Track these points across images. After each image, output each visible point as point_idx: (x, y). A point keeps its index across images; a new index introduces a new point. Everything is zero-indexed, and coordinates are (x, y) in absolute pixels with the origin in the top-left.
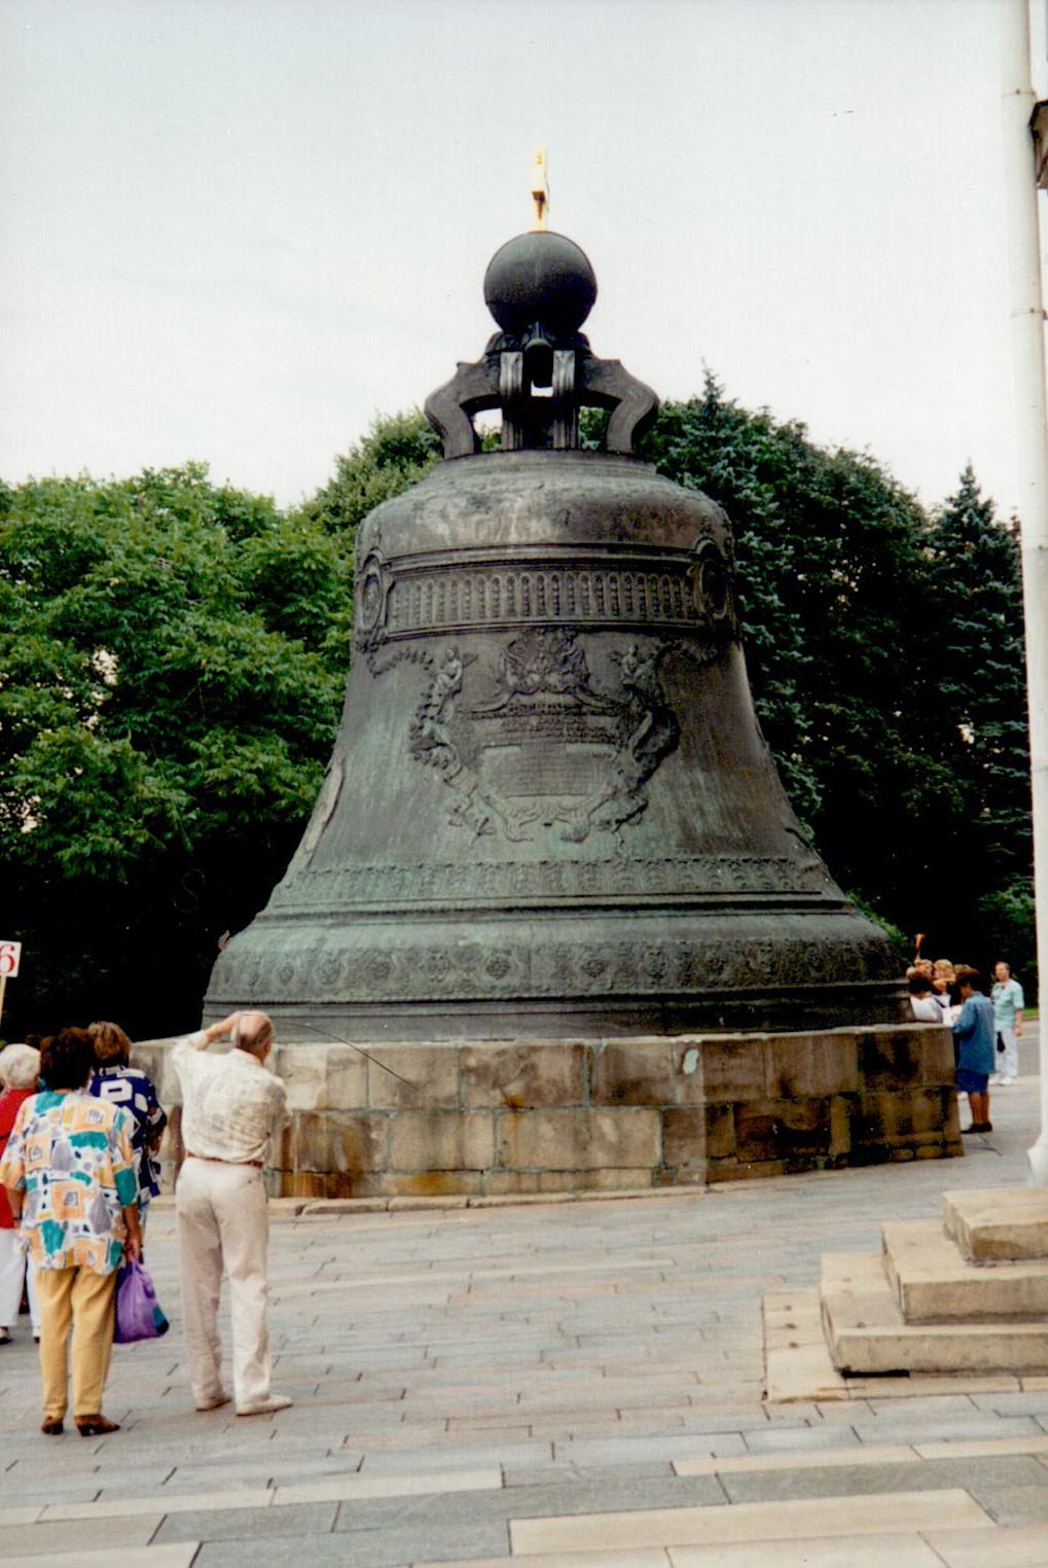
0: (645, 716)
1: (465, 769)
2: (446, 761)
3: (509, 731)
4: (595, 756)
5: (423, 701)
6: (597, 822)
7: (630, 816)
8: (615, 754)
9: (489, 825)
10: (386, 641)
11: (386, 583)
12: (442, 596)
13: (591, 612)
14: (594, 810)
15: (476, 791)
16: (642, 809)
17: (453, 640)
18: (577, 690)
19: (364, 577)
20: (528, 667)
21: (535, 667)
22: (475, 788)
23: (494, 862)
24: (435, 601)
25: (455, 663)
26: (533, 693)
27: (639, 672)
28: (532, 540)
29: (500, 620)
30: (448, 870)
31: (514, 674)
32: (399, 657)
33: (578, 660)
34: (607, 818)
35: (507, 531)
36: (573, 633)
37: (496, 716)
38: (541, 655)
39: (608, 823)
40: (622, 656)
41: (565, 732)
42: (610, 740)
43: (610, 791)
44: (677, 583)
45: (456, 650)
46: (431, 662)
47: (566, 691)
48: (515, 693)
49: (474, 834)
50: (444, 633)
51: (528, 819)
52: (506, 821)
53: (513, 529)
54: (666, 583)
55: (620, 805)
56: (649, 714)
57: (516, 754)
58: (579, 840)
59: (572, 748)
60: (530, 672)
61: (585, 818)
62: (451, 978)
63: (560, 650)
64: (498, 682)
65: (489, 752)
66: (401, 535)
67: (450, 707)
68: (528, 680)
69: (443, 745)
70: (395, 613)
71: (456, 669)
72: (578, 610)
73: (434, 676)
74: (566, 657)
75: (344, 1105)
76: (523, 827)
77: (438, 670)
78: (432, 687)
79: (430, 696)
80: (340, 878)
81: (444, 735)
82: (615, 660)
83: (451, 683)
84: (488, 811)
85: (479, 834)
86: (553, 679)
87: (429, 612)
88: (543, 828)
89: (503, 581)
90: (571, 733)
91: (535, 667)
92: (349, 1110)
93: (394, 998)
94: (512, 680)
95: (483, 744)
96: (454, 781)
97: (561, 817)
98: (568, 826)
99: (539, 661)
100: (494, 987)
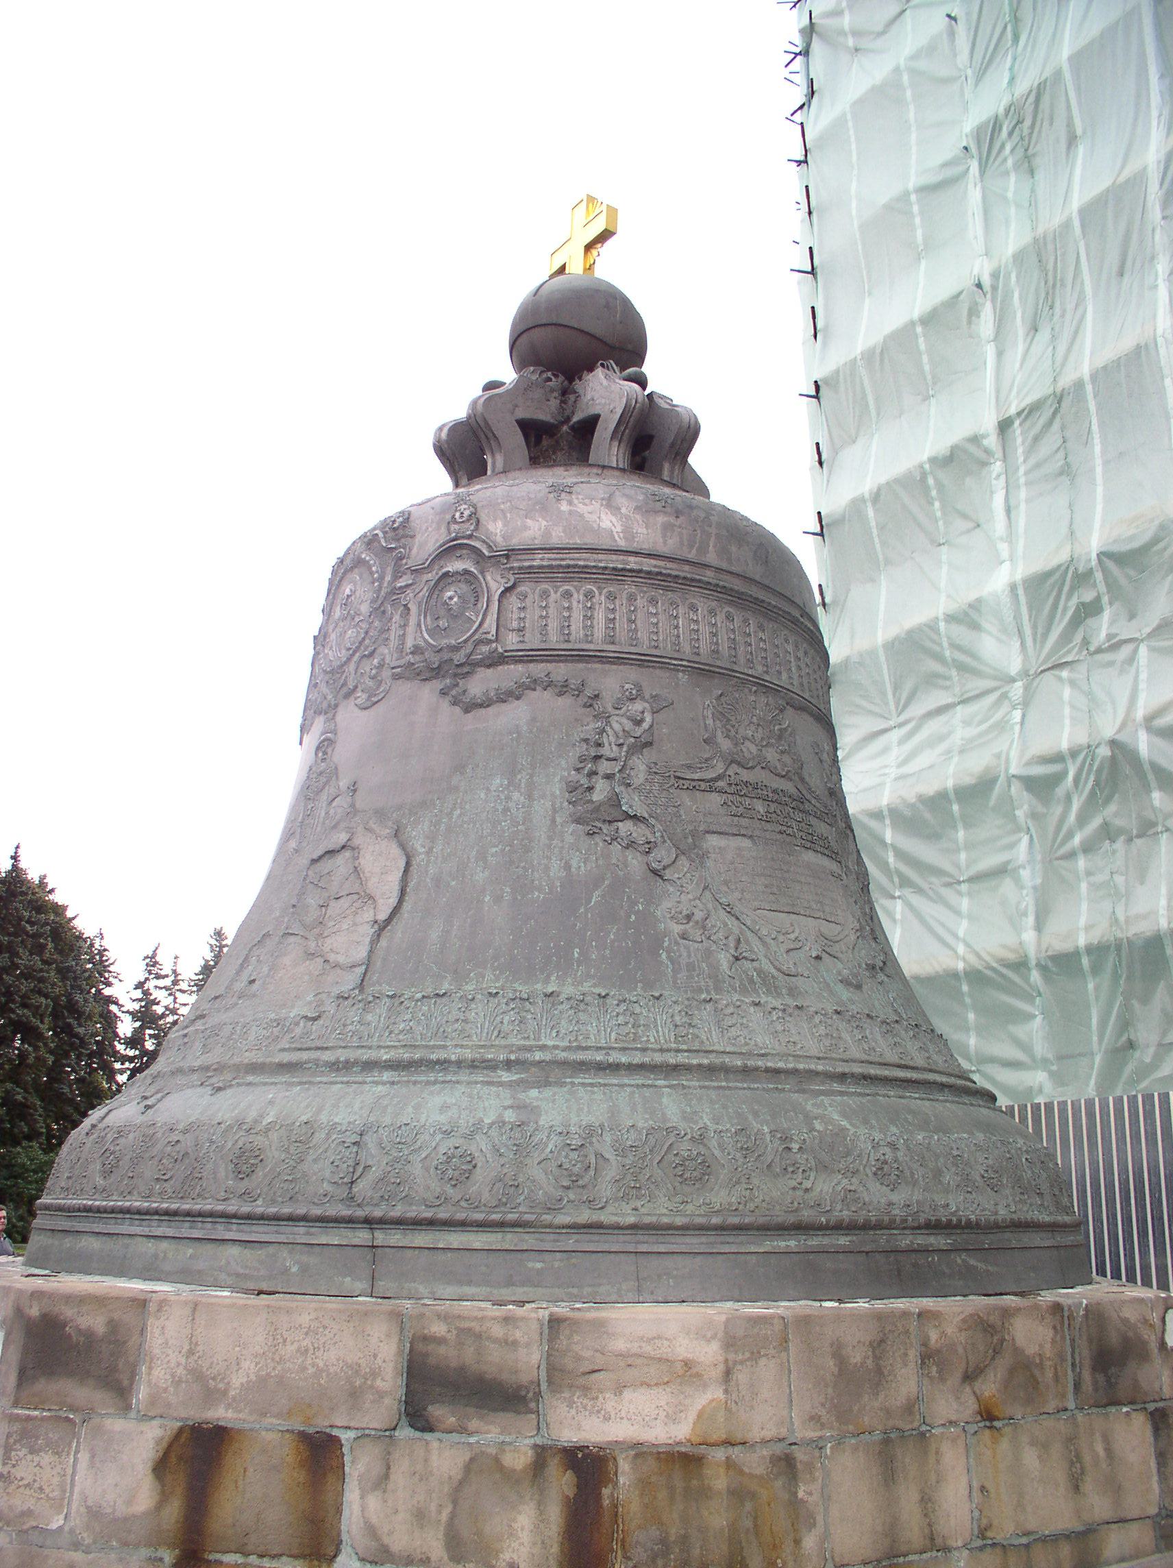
1: (683, 861)
9: (743, 946)
11: (494, 582)
12: (613, 610)
17: (631, 673)
18: (796, 778)
19: (432, 576)
21: (750, 733)
24: (600, 616)
25: (638, 706)
26: (752, 768)
28: (733, 569)
30: (709, 1007)
35: (703, 550)
37: (711, 790)
46: (597, 696)
48: (732, 762)
52: (765, 944)
59: (809, 856)
62: (824, 1187)
65: (713, 841)
66: (529, 522)
67: (639, 766)
68: (744, 750)
70: (515, 625)
71: (643, 712)
72: (784, 676)
75: (756, 1434)
77: (610, 709)
80: (478, 1011)
81: (633, 803)
83: (638, 732)
84: (731, 922)
85: (737, 959)
86: (771, 755)
91: (750, 733)
92: (765, 1442)
93: (735, 1220)
94: (725, 744)
97: (828, 950)
100: (890, 1204)
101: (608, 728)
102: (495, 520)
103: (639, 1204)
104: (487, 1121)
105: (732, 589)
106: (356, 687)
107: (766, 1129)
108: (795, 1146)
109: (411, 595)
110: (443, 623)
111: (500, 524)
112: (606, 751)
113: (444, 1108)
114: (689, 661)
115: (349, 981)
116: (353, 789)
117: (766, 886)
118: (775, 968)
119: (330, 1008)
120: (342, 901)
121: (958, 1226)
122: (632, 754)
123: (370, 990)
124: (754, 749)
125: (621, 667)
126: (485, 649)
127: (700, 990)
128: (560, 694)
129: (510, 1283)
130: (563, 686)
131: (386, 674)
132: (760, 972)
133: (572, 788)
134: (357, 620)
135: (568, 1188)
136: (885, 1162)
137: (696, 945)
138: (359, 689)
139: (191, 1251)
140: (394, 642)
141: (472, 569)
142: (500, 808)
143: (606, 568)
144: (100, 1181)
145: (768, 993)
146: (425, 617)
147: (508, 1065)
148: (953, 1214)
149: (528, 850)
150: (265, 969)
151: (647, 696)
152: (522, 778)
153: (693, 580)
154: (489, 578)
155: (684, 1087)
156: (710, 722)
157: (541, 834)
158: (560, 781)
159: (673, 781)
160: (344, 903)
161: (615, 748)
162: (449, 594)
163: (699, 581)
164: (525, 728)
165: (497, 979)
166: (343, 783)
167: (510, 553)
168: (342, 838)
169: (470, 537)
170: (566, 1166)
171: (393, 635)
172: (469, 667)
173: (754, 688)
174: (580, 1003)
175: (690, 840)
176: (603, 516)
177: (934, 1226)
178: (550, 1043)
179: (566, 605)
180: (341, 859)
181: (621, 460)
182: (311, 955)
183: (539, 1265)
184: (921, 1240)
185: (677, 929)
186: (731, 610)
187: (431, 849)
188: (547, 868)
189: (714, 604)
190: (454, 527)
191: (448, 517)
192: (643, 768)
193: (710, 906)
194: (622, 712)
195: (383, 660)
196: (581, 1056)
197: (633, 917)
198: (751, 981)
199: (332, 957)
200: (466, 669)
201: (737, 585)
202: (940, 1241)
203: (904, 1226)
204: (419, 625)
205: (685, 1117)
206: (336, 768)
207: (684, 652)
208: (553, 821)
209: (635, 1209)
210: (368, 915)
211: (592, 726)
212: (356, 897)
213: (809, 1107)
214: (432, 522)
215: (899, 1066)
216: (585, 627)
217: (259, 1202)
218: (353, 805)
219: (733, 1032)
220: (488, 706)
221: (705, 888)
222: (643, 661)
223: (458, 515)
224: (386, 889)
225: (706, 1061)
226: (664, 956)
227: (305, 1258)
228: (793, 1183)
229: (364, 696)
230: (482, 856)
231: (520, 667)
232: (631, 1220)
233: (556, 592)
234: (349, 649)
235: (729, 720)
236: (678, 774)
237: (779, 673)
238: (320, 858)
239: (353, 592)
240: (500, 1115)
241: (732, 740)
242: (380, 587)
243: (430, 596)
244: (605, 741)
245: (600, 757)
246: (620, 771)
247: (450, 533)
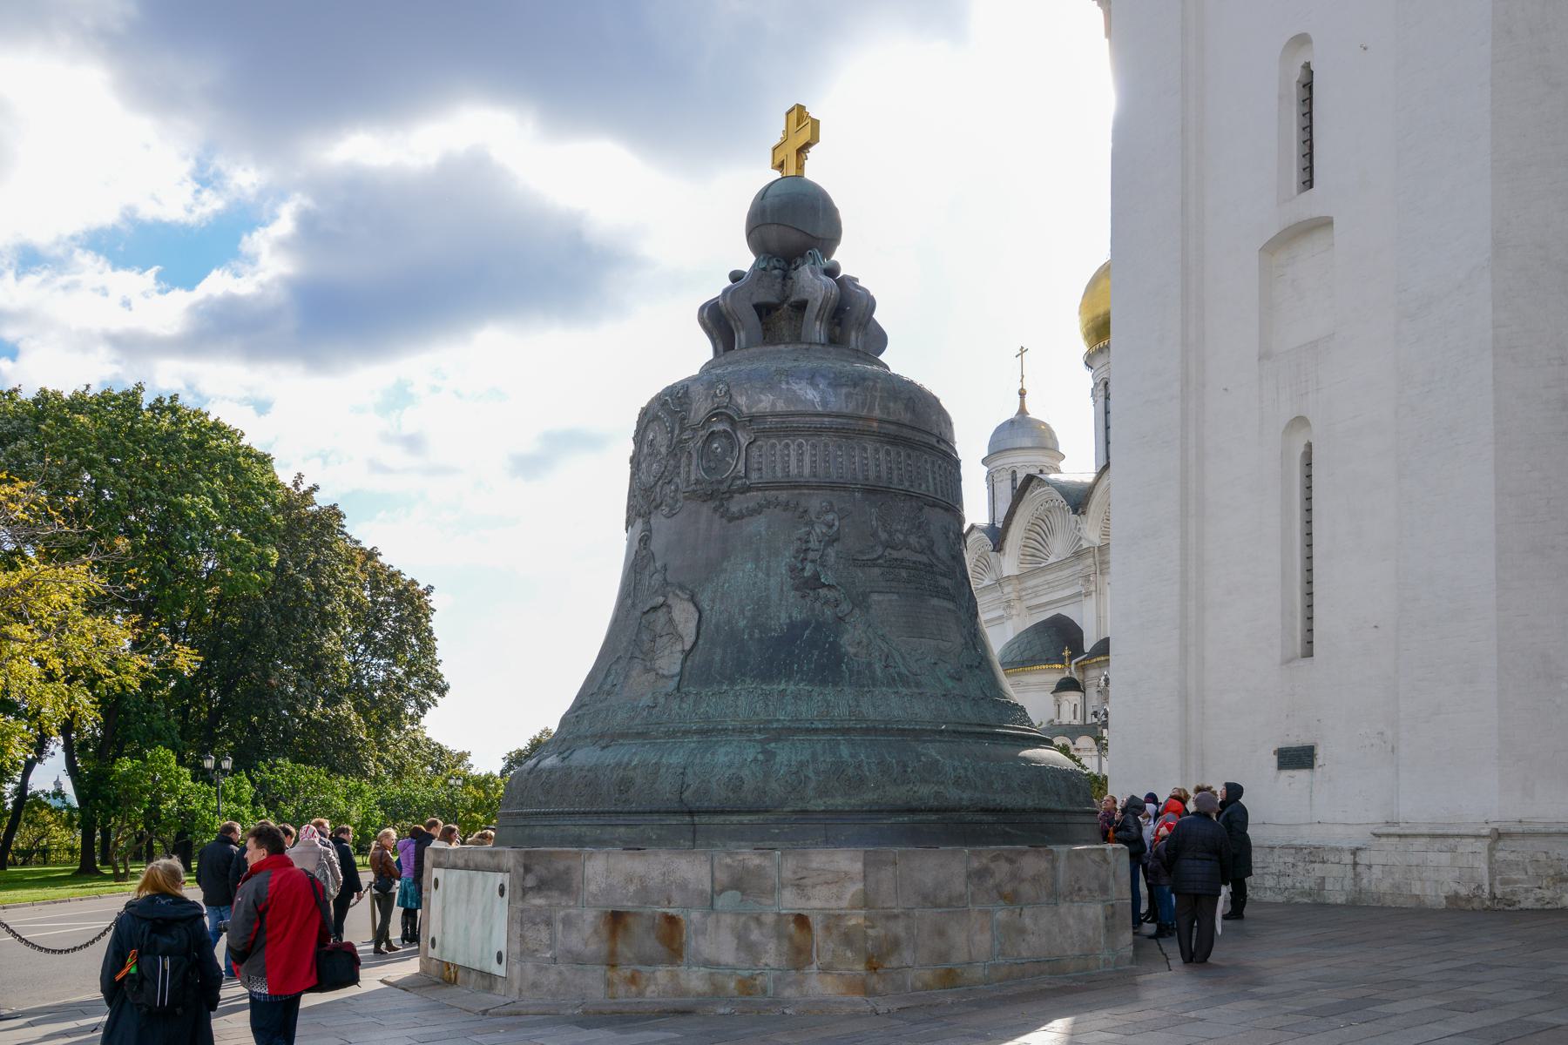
10: (746, 489)
12: (815, 455)
24: (807, 459)
25: (830, 517)
31: (885, 531)
35: (871, 409)
37: (875, 565)
45: (831, 504)
46: (806, 511)
48: (887, 547)
52: (903, 658)
53: (877, 407)
59: (935, 601)
62: (925, 791)
65: (875, 597)
69: (830, 587)
70: (756, 466)
71: (833, 520)
72: (924, 486)
73: (811, 524)
77: (813, 518)
78: (809, 533)
79: (807, 542)
80: (742, 701)
83: (831, 532)
85: (886, 667)
86: (913, 540)
89: (870, 448)
94: (884, 536)
95: (868, 590)
99: (901, 523)
100: (961, 799)
101: (813, 532)
102: (741, 395)
103: (827, 799)
104: (749, 760)
105: (889, 434)
106: (661, 503)
107: (894, 761)
108: (910, 770)
109: (692, 445)
110: (712, 465)
111: (744, 399)
112: (811, 545)
113: (727, 754)
114: (862, 485)
115: (672, 684)
116: (665, 568)
118: (909, 671)
119: (662, 700)
120: (664, 638)
121: (1000, 810)
123: (683, 690)
124: (901, 537)
125: (820, 492)
126: (739, 482)
127: (864, 686)
128: (784, 510)
129: (762, 840)
131: (680, 496)
132: (899, 674)
133: (792, 569)
134: (659, 458)
135: (790, 792)
136: (960, 778)
138: (664, 504)
139: (599, 831)
140: (683, 475)
141: (729, 429)
142: (751, 582)
143: (809, 427)
144: (542, 798)
145: (903, 686)
146: (702, 460)
147: (759, 730)
148: (999, 804)
149: (768, 607)
150: (622, 678)
151: (836, 509)
152: (763, 564)
153: (864, 431)
154: (739, 435)
155: (853, 740)
156: (874, 523)
157: (775, 597)
158: (785, 565)
159: (851, 562)
160: (665, 639)
161: (817, 543)
162: (715, 445)
163: (868, 431)
164: (764, 532)
165: (752, 683)
166: (659, 564)
167: (752, 419)
168: (661, 600)
169: (726, 407)
170: (790, 781)
171: (682, 471)
172: (730, 493)
173: (903, 498)
174: (797, 697)
175: (861, 598)
176: (808, 391)
177: (985, 811)
178: (782, 718)
179: (786, 452)
180: (661, 613)
181: (822, 338)
182: (647, 670)
183: (777, 831)
184: (977, 817)
186: (889, 447)
187: (712, 608)
188: (779, 618)
189: (878, 445)
190: (716, 400)
191: (712, 392)
192: (833, 554)
193: (872, 637)
194: (820, 521)
195: (678, 486)
196: (797, 725)
197: (827, 645)
198: (894, 680)
199: (661, 672)
200: (727, 495)
201: (892, 429)
202: (990, 818)
203: (967, 809)
204: (698, 465)
205: (852, 756)
206: (653, 554)
208: (782, 590)
209: (825, 803)
210: (679, 648)
211: (803, 530)
212: (671, 636)
213: (920, 749)
214: (702, 394)
215: (979, 725)
216: (798, 466)
217: (634, 805)
218: (665, 579)
219: (881, 709)
220: (743, 518)
221: (869, 626)
222: (832, 486)
223: (718, 391)
224: (688, 629)
225: (864, 726)
226: (844, 667)
227: (659, 832)
228: (908, 788)
229: (667, 509)
230: (742, 611)
231: (760, 493)
232: (823, 808)
233: (780, 444)
234: (655, 477)
237: (920, 485)
238: (648, 611)
239: (655, 438)
240: (756, 757)
242: (672, 436)
243: (703, 447)
244: (812, 539)
245: (808, 549)
247: (713, 404)
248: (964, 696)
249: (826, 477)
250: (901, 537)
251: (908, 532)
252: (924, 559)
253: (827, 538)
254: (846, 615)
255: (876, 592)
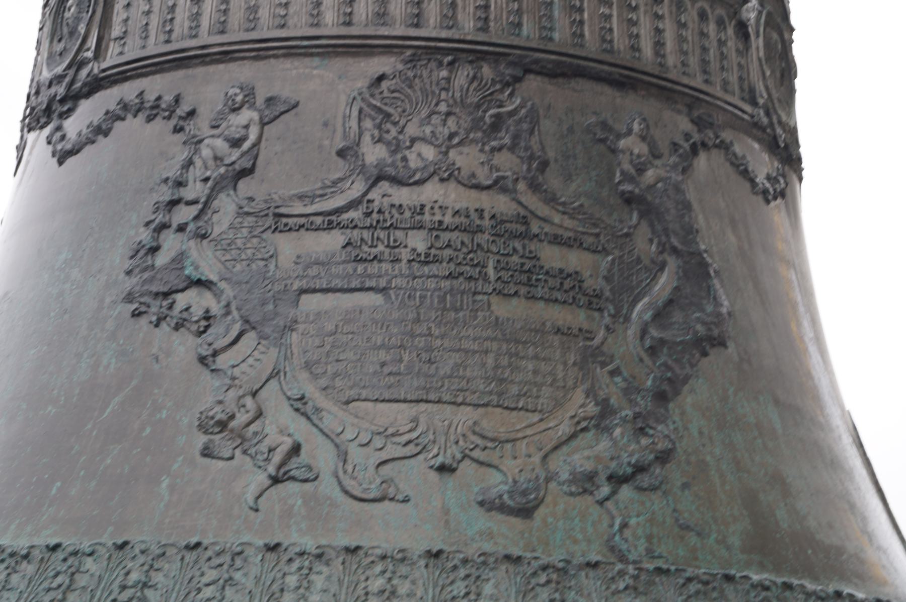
0: (662, 267)
1: (250, 339)
2: (207, 317)
3: (359, 260)
4: (558, 331)
5: (165, 194)
6: (565, 476)
7: (640, 469)
8: (602, 333)
10: (96, 85)
13: (556, 36)
14: (556, 448)
15: (273, 383)
16: (664, 457)
18: (521, 186)
20: (412, 130)
21: (428, 130)
22: (275, 374)
23: (310, 544)
27: (650, 175)
29: (354, 31)
32: (125, 110)
33: (525, 126)
34: (589, 466)
36: (519, 72)
37: (330, 226)
38: (443, 107)
39: (591, 477)
40: (619, 136)
41: (491, 271)
42: (594, 302)
43: (592, 409)
44: (720, 23)
46: (192, 114)
47: (498, 185)
48: (379, 179)
49: (261, 478)
50: (226, 56)
51: (400, 452)
54: (703, 16)
55: (615, 443)
56: (672, 263)
57: (375, 309)
58: (525, 512)
59: (502, 309)
60: (413, 141)
61: (537, 459)
63: (487, 100)
64: (341, 153)
65: (311, 303)
67: (226, 204)
68: (412, 156)
71: (247, 127)
74: (498, 116)
76: (386, 470)
78: (189, 163)
82: (603, 141)
84: (300, 428)
85: (275, 480)
87: (196, 17)
88: (433, 476)
90: (505, 275)
96: (222, 361)
97: (476, 454)
98: (495, 477)
99: (436, 120)
117: (383, 365)
122: (219, 192)
128: (150, 119)
130: (152, 108)
137: (221, 464)
151: (260, 101)
159: (270, 221)
185: (201, 439)
197: (148, 430)
207: (326, 25)
226: (164, 485)
235: (388, 115)
236: (282, 210)
241: (388, 144)
246: (197, 218)
248: (507, 557)
249: (247, 30)
250: (429, 153)
251: (456, 140)
252: (501, 204)
253: (222, 170)
254: (215, 354)
255: (315, 291)
